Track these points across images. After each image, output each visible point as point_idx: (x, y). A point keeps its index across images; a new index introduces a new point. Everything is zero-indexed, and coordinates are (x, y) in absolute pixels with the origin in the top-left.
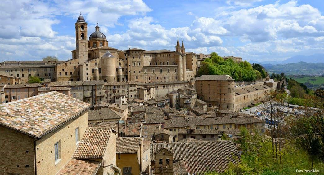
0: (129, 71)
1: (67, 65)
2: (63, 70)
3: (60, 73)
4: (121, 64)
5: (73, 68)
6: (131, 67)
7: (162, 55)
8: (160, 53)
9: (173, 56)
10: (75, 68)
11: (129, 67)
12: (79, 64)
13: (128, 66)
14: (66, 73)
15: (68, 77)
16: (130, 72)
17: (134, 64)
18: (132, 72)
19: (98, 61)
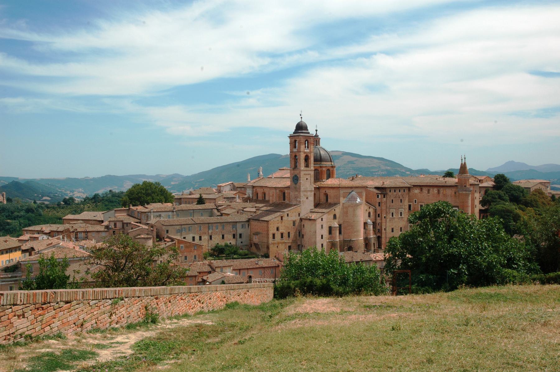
0: (383, 227)
1: (284, 218)
2: (278, 229)
3: (274, 235)
4: (372, 214)
5: (292, 225)
6: (388, 220)
7: (425, 190)
8: (420, 186)
9: (453, 193)
10: (294, 223)
11: (384, 220)
12: (301, 215)
13: (383, 217)
14: (282, 234)
15: (284, 243)
16: (385, 229)
17: (392, 213)
18: (389, 230)
19: (338, 210)
